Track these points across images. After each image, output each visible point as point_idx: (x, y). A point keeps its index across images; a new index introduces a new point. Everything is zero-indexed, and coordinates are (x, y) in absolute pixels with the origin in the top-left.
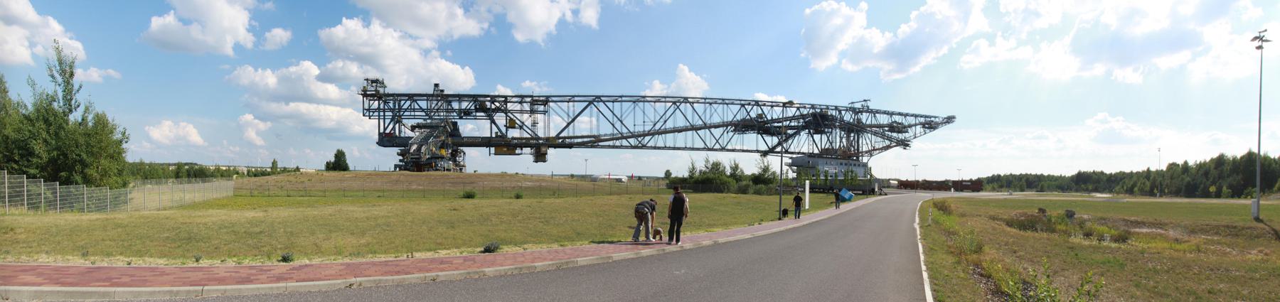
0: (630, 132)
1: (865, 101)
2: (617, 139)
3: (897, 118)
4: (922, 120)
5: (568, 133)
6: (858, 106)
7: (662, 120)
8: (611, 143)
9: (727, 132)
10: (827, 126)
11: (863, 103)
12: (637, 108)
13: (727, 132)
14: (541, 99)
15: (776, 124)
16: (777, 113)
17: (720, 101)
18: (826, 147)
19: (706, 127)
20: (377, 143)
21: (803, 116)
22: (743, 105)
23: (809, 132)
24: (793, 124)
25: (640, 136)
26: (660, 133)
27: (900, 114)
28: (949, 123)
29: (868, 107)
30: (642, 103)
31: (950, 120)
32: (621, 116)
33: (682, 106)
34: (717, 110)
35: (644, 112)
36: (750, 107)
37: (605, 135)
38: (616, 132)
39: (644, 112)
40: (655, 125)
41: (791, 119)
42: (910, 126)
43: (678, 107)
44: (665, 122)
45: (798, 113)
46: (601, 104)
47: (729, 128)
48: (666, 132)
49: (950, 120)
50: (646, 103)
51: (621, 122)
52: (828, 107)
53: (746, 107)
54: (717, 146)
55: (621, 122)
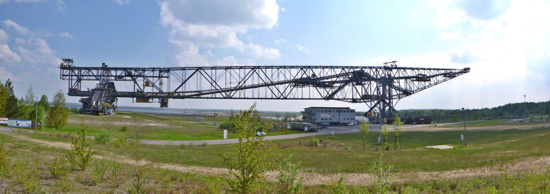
0: (221, 89)
1: (393, 62)
2: (213, 93)
3: (422, 72)
4: (443, 72)
5: (182, 90)
6: (389, 65)
7: (243, 81)
8: (210, 96)
9: (291, 87)
10: (365, 80)
11: (392, 63)
12: (227, 72)
13: (291, 87)
14: (166, 69)
15: (325, 80)
16: (328, 72)
17: (284, 67)
18: (363, 94)
19: (272, 84)
20: (68, 94)
21: (347, 74)
22: (302, 69)
23: (353, 84)
24: (338, 80)
25: (228, 91)
26: (241, 88)
27: (422, 69)
28: (465, 73)
29: (396, 66)
30: (229, 70)
31: (466, 70)
32: (216, 80)
33: (257, 71)
34: (306, 72)
35: (230, 74)
36: (306, 69)
37: (206, 91)
38: (213, 88)
39: (230, 74)
40: (239, 83)
41: (337, 76)
42: (432, 77)
43: (255, 71)
44: (245, 82)
45: (343, 72)
46: (202, 70)
47: (291, 83)
48: (245, 88)
49: (466, 70)
50: (232, 70)
51: (216, 83)
52: (365, 68)
53: (304, 69)
54: (282, 97)
55: (216, 83)
